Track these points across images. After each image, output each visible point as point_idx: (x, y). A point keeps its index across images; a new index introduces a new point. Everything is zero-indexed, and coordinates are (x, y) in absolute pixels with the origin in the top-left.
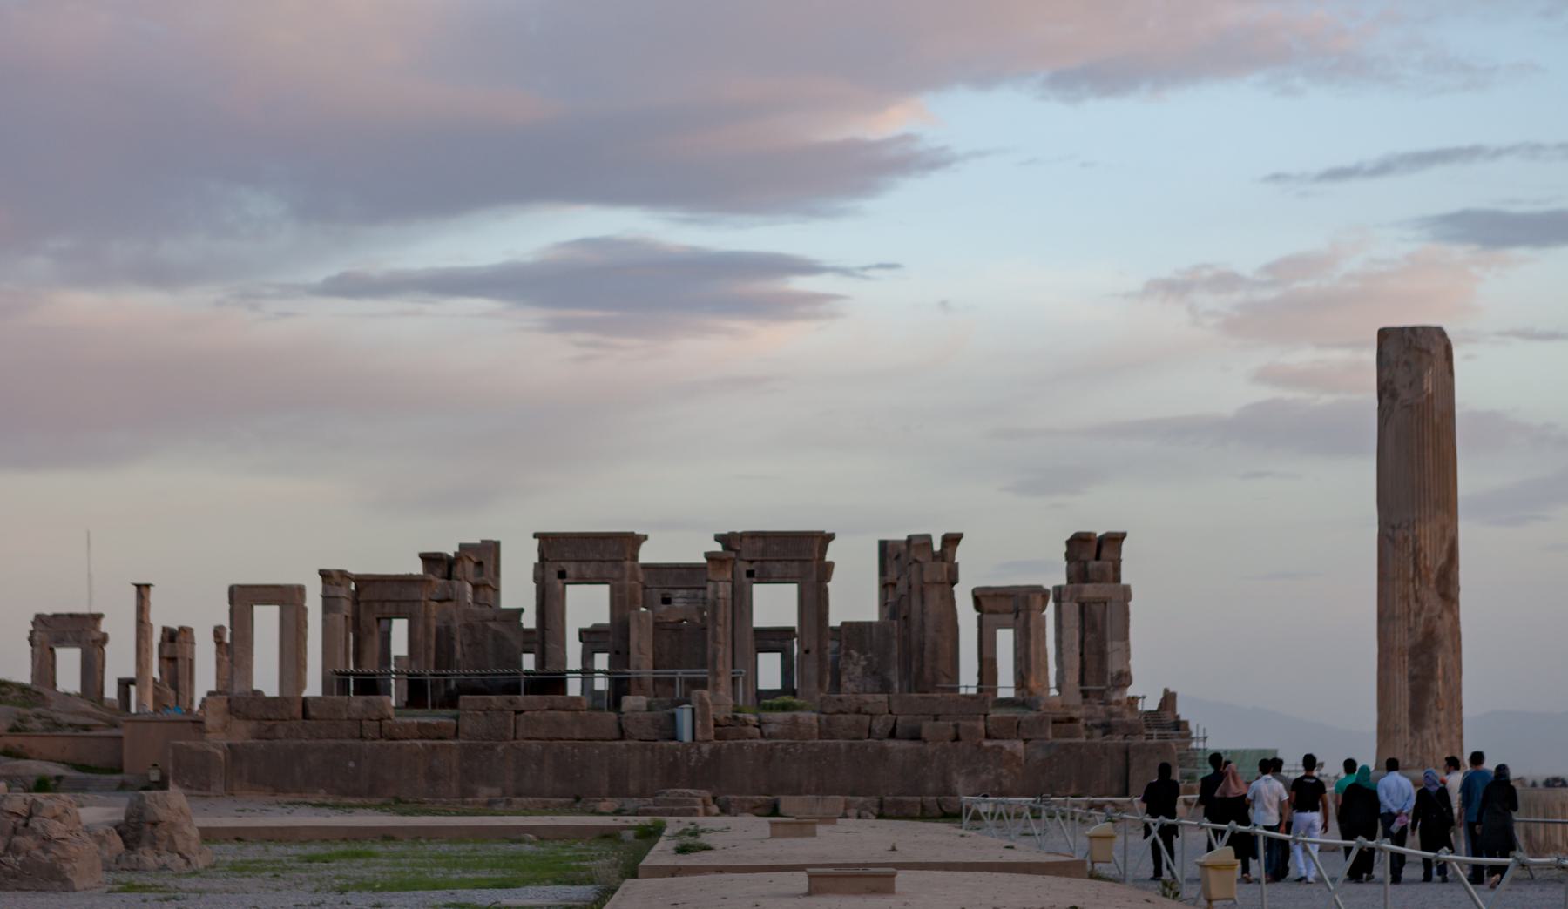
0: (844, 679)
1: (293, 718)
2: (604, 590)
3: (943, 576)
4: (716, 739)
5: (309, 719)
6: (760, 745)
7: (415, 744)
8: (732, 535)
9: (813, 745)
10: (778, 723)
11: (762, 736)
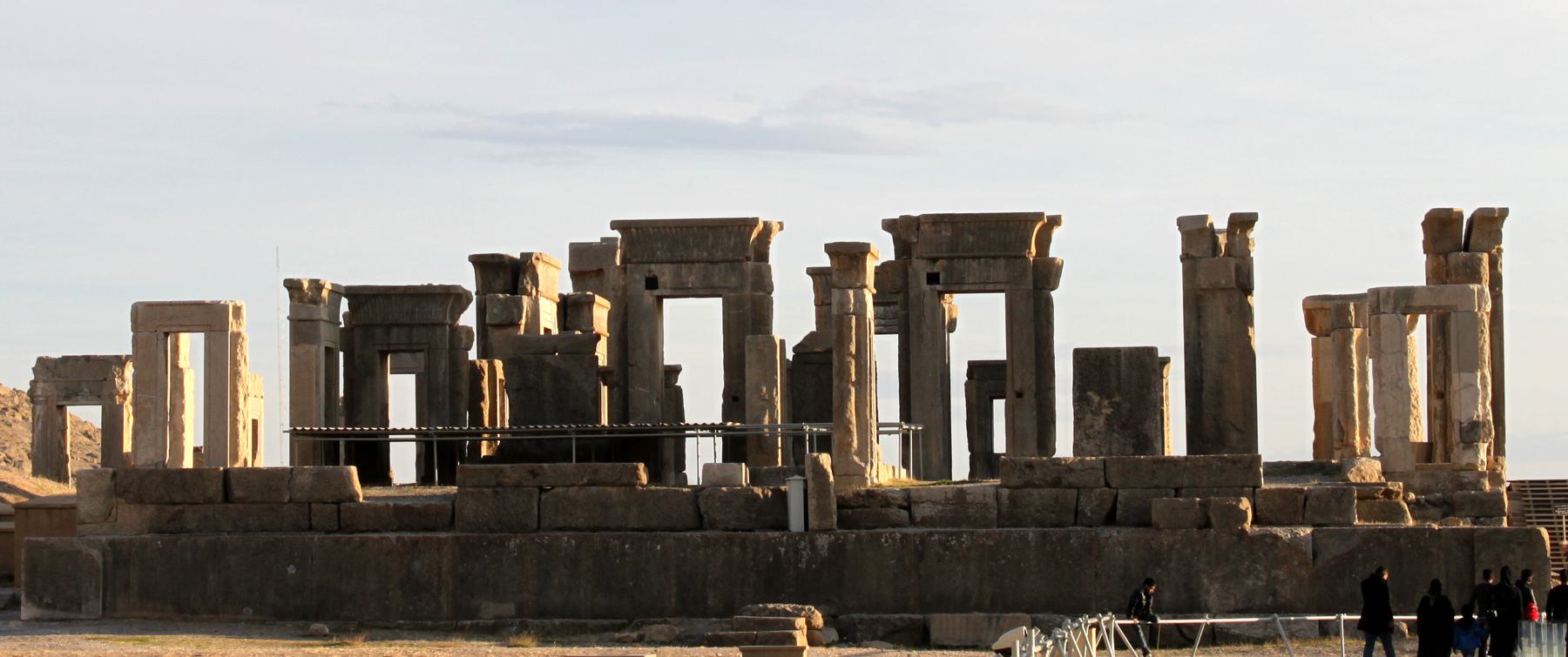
1: (209, 501)
2: (716, 304)
3: (1227, 279)
4: (839, 527)
5: (233, 502)
6: (905, 536)
7: (387, 539)
8: (906, 220)
9: (988, 536)
10: (935, 503)
11: (912, 521)
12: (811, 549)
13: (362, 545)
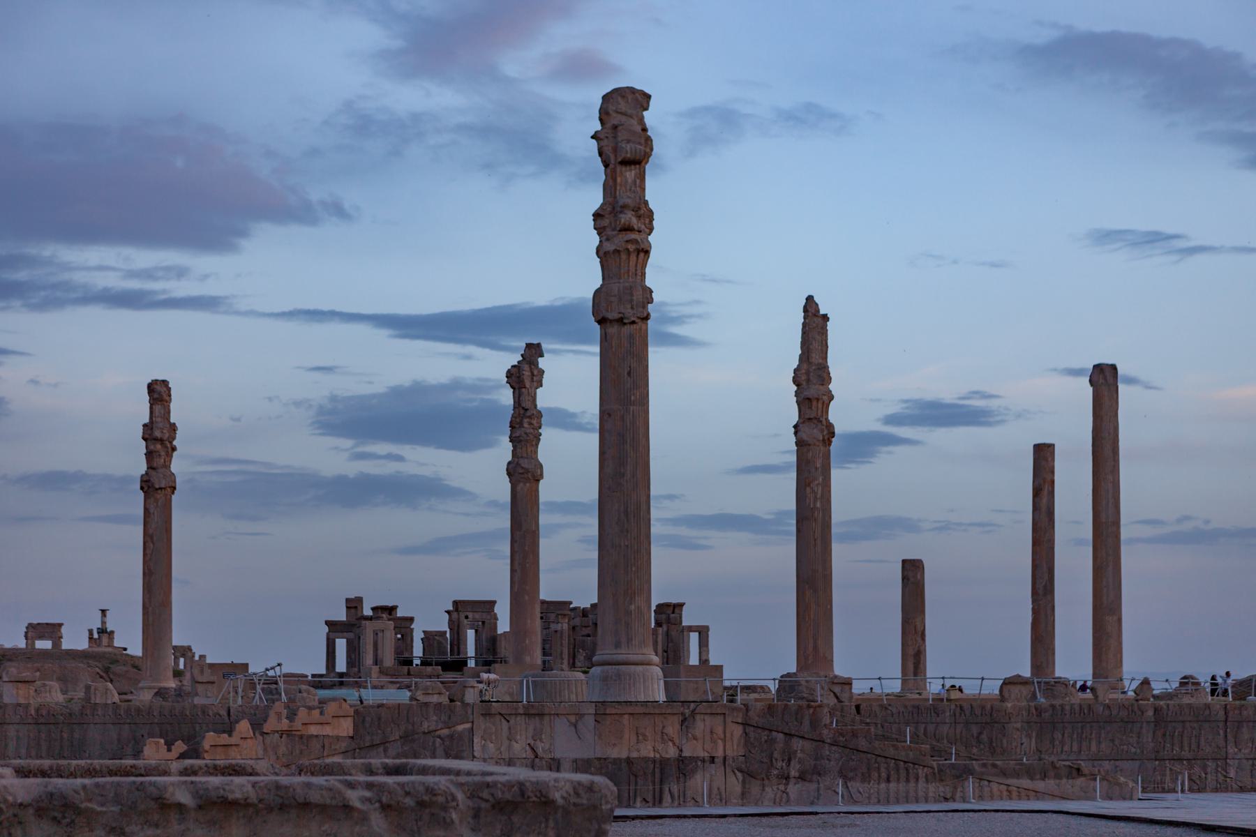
0: (576, 661)
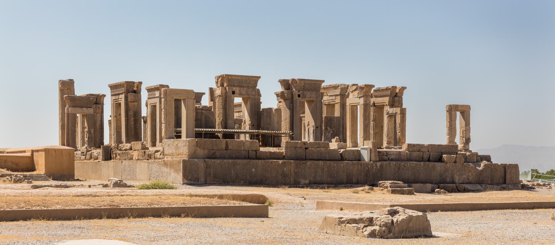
12: (376, 166)
13: (272, 163)
